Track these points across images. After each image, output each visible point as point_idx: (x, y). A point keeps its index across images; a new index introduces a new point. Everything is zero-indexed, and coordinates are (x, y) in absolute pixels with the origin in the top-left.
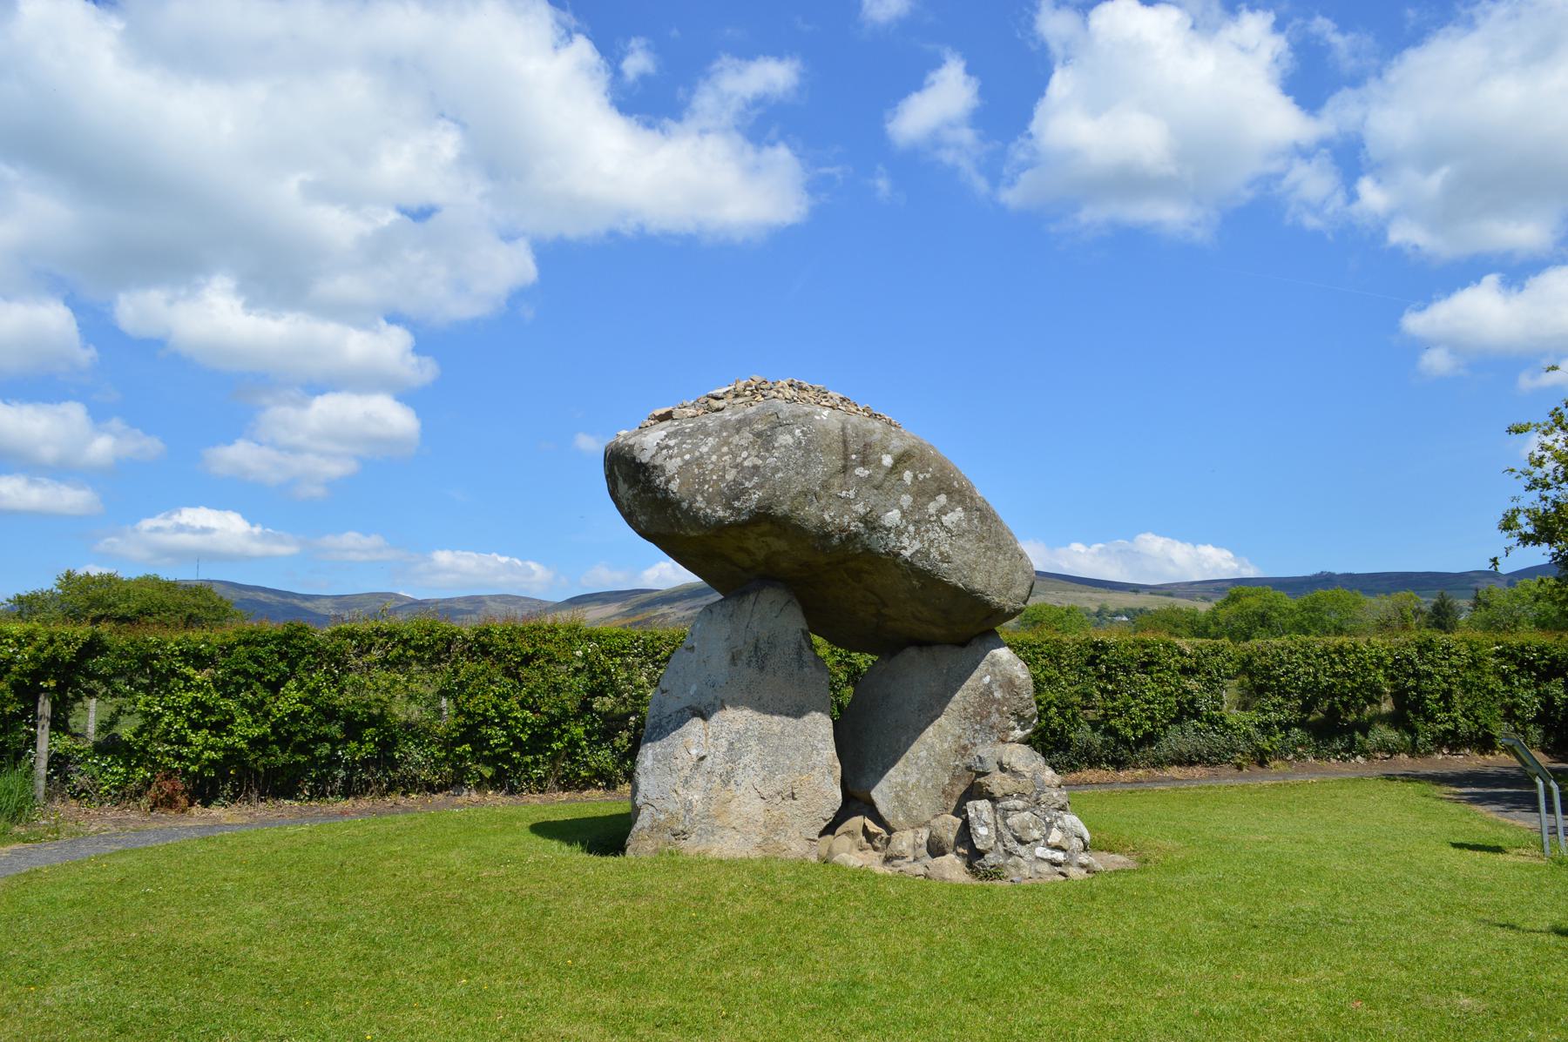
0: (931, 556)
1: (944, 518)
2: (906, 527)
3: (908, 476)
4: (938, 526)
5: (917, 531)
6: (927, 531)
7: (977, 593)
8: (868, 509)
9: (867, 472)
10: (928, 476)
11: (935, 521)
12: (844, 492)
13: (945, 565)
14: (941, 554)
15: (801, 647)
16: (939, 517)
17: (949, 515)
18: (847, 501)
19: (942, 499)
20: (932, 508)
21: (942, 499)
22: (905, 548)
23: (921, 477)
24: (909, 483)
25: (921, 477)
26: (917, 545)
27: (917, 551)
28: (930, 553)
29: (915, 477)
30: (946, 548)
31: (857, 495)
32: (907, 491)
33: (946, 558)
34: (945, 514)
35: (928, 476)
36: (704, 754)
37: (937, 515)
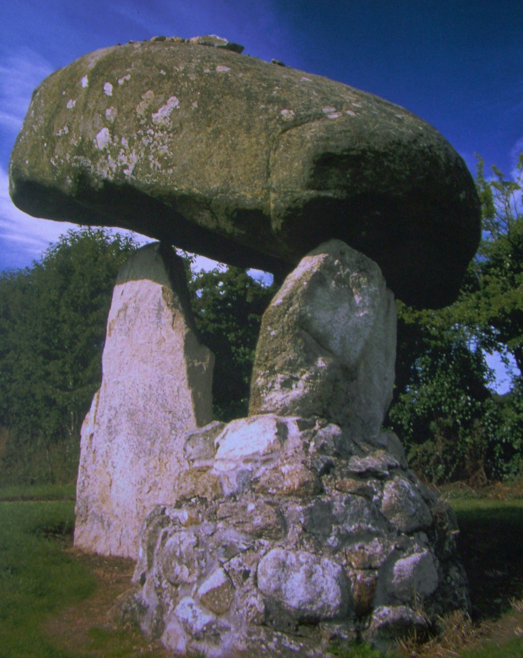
0: (151, 166)
1: (154, 116)
2: (119, 143)
3: (109, 88)
4: (151, 128)
5: (131, 142)
6: (140, 138)
7: (217, 194)
8: (80, 138)
9: (74, 102)
10: (128, 77)
11: (147, 124)
12: (60, 131)
13: (171, 171)
14: (161, 160)
15: (160, 309)
16: (149, 118)
17: (160, 111)
18: (66, 138)
19: (149, 94)
20: (141, 109)
21: (149, 94)
22: (126, 167)
23: (121, 82)
24: (111, 94)
25: (121, 82)
26: (134, 158)
27: (136, 166)
28: (149, 162)
29: (115, 85)
30: (164, 150)
31: (70, 130)
32: (111, 101)
33: (166, 163)
34: (156, 111)
35: (128, 77)
36: (92, 431)
37: (147, 117)
